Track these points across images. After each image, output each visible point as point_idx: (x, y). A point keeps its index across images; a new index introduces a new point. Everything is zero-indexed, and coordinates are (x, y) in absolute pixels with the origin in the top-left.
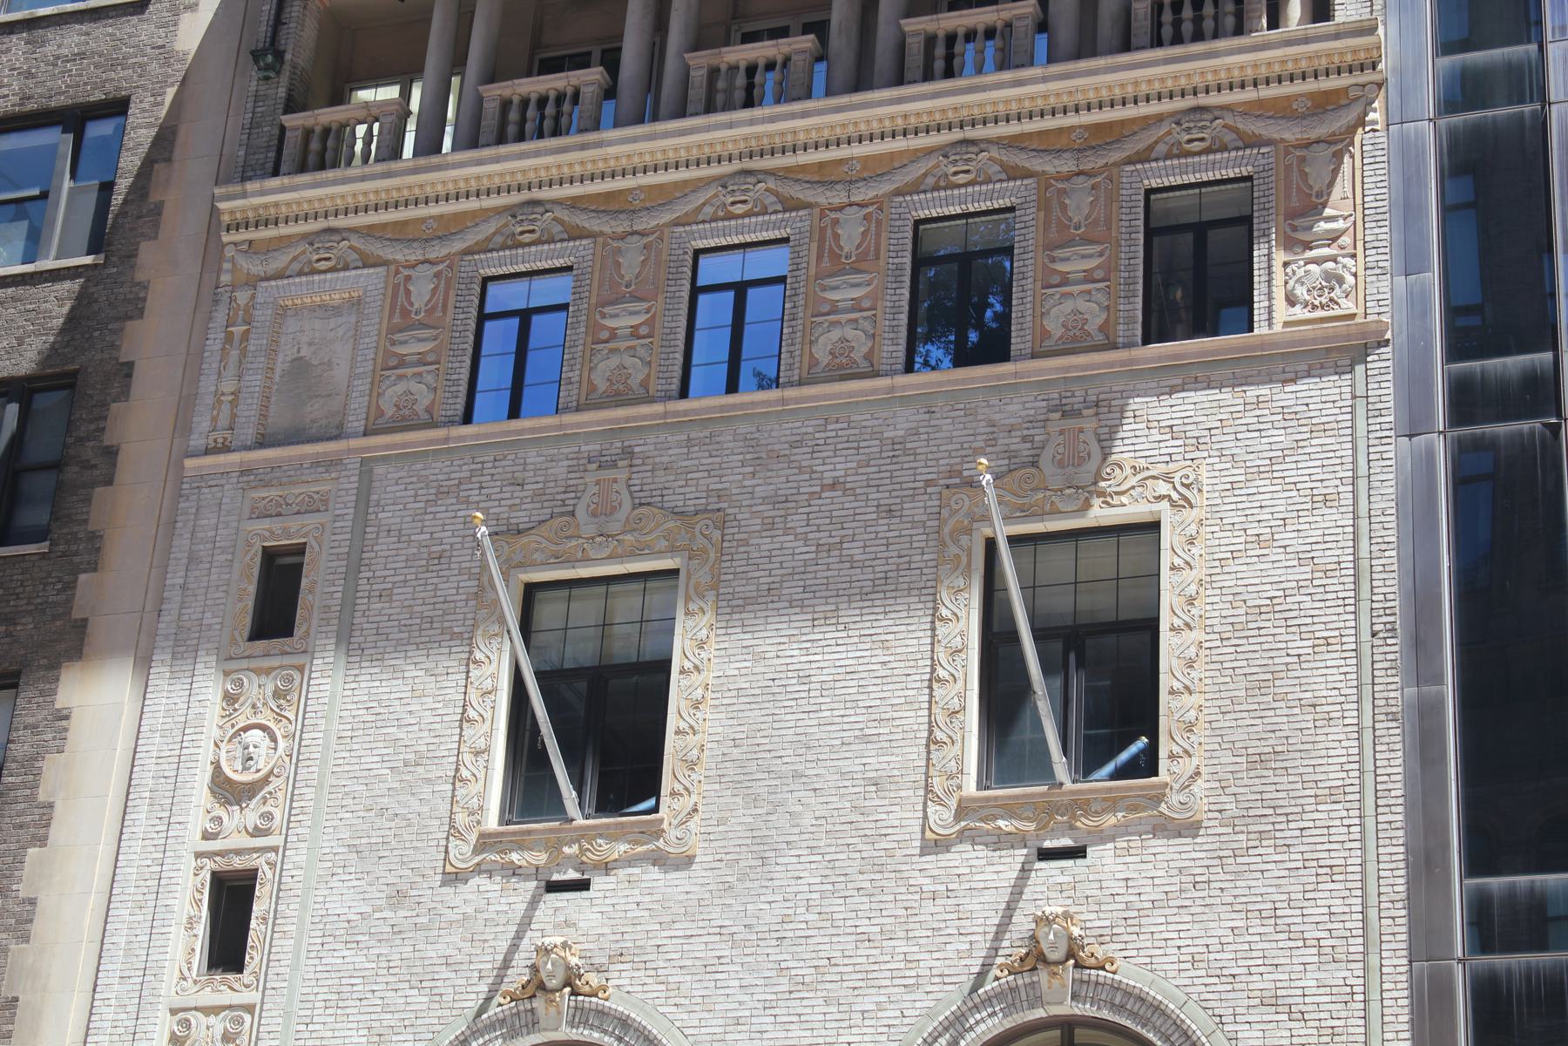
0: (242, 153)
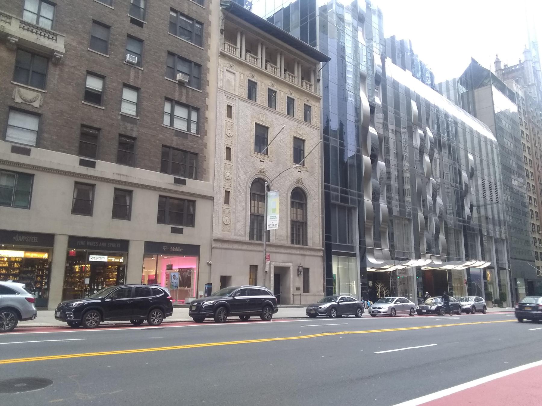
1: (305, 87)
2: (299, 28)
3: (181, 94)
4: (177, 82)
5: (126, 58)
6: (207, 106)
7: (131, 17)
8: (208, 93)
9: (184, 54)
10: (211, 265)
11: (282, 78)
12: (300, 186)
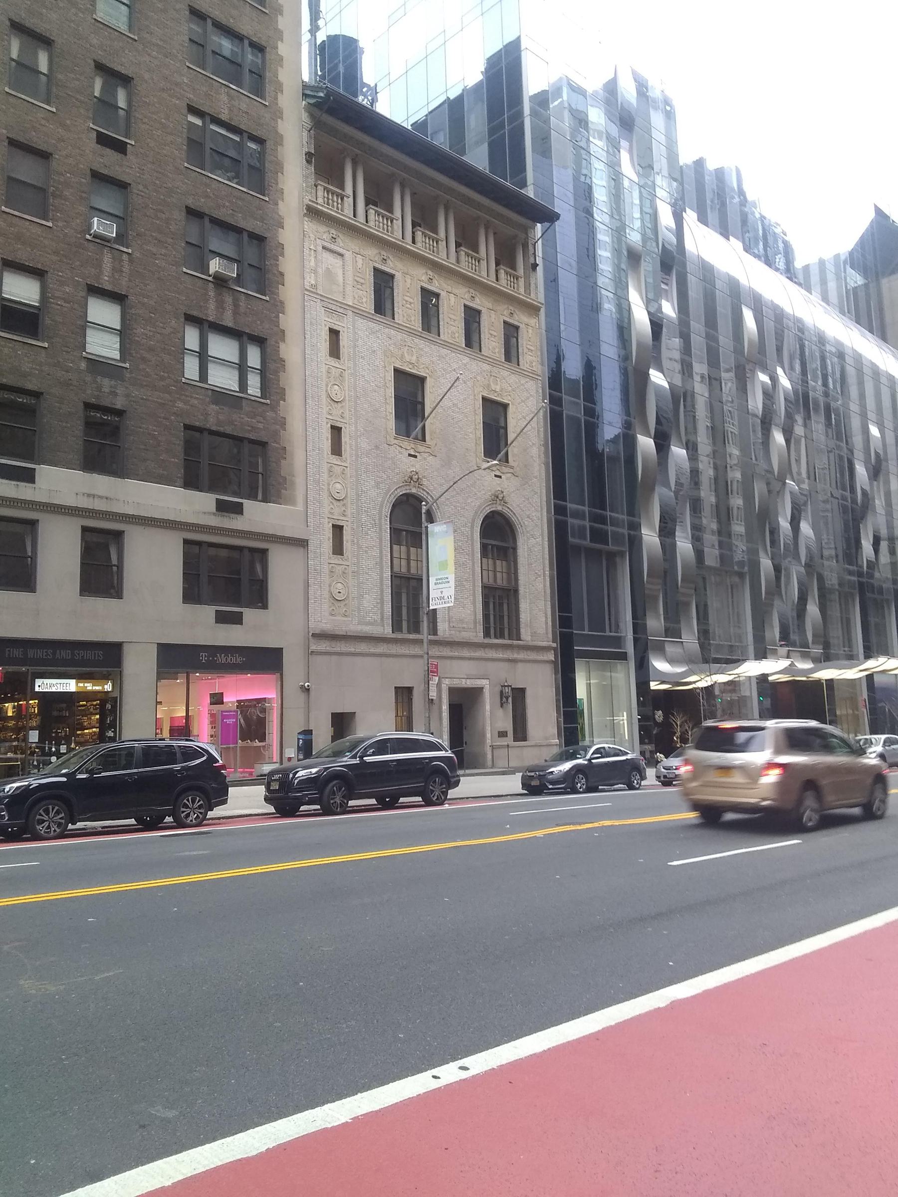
0: (304, 185)
1: (504, 284)
2: (486, 145)
3: (220, 305)
4: (210, 279)
5: (90, 226)
6: (283, 332)
7: (97, 131)
8: (282, 303)
9: (222, 214)
10: (307, 690)
11: (451, 263)
12: (499, 508)
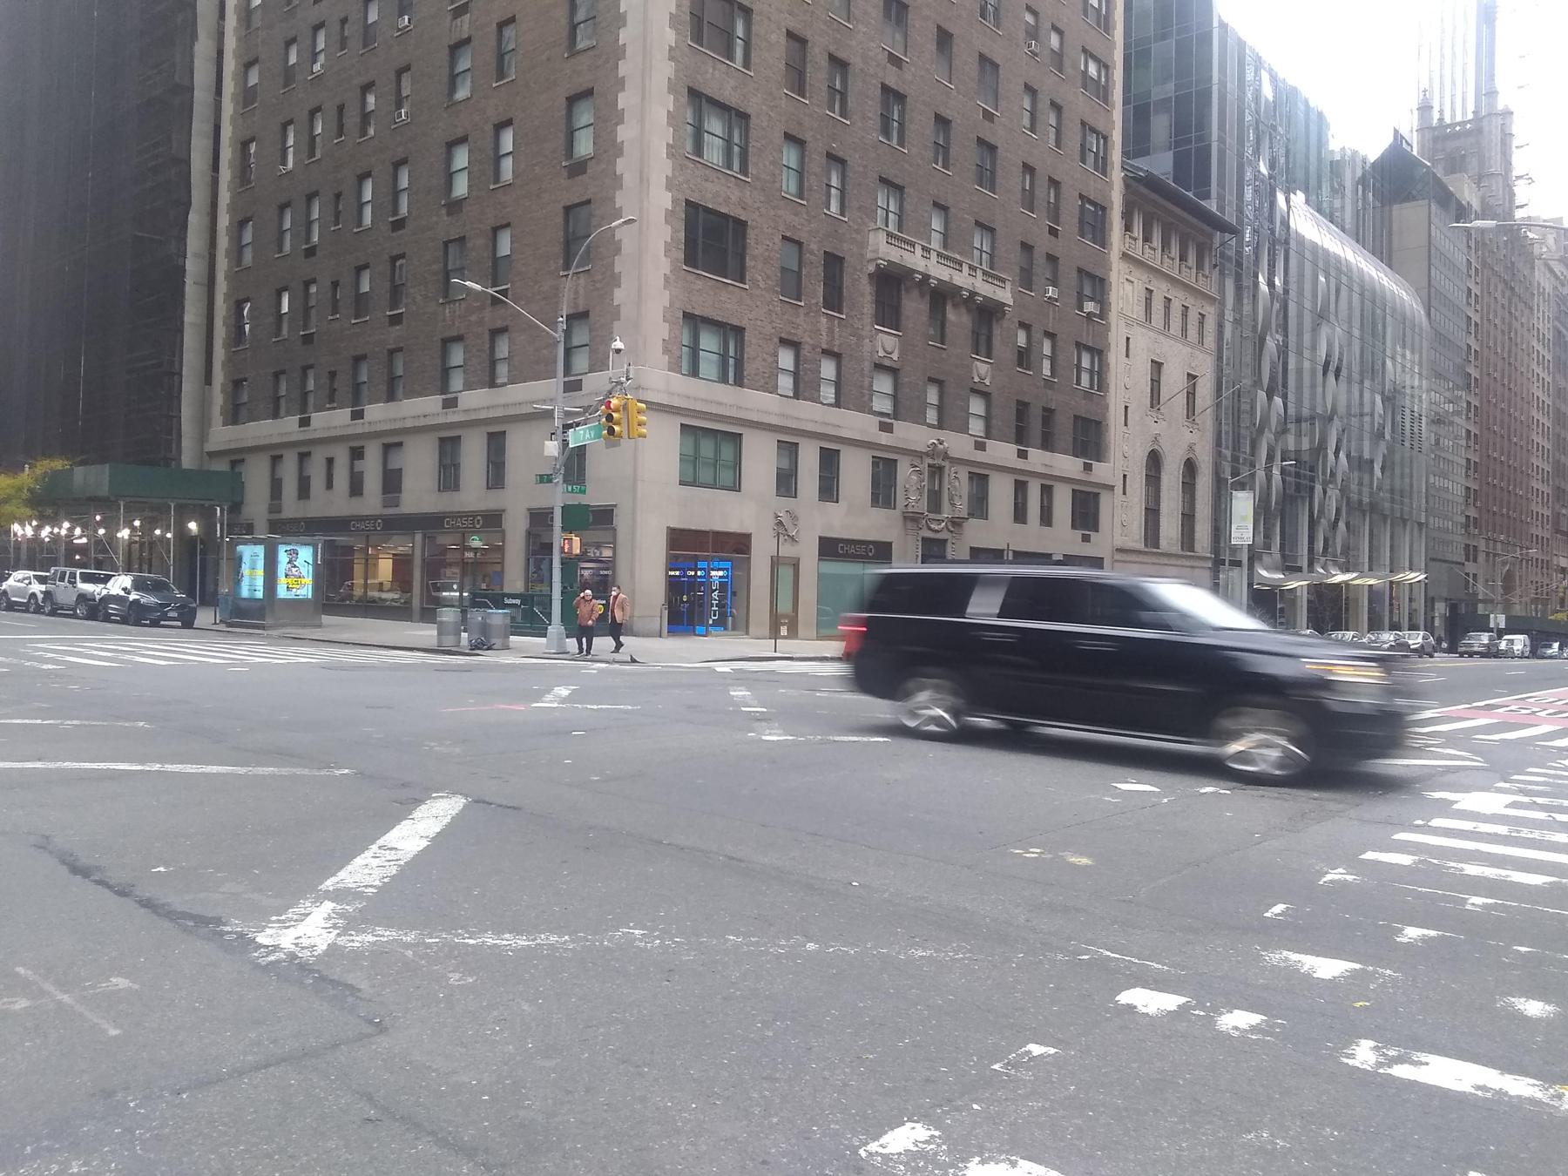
4: (1085, 315)
5: (1046, 291)
11: (1156, 264)
